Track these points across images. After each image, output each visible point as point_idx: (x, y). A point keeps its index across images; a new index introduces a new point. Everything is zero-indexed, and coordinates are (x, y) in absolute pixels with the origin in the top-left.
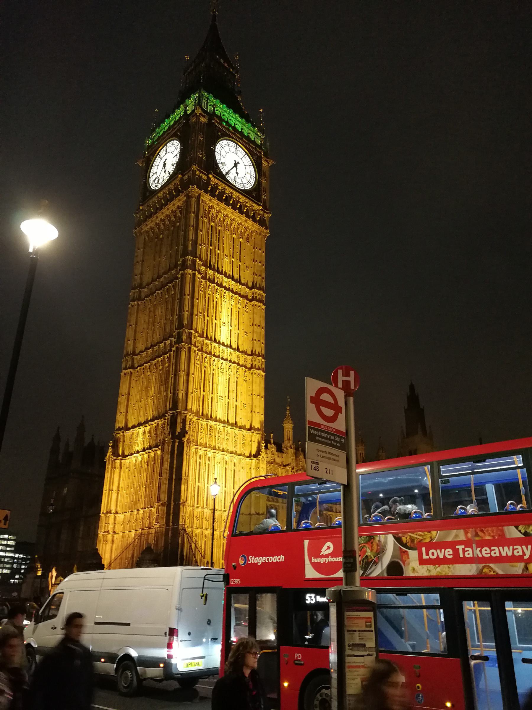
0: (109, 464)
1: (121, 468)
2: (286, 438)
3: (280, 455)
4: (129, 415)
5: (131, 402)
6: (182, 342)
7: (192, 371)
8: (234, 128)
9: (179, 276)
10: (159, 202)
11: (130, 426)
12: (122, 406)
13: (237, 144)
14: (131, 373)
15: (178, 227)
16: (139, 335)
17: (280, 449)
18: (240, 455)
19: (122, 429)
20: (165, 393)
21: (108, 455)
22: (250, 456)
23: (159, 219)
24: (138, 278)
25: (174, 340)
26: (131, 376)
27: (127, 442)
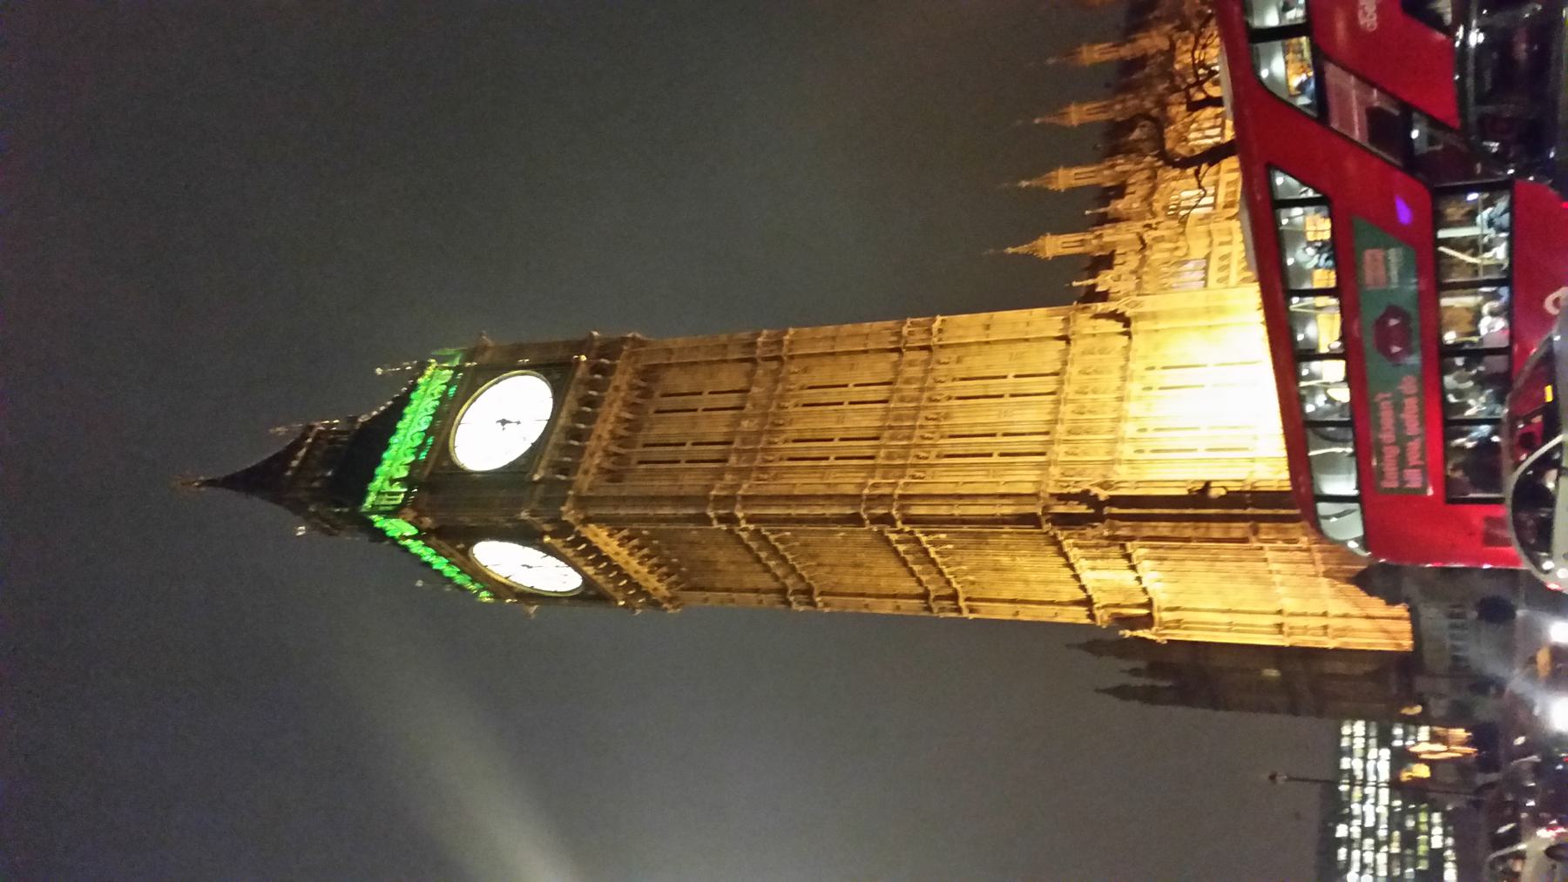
3: (1118, 260)
7: (950, 490)
8: (428, 433)
9: (752, 527)
17: (1105, 261)
18: (1127, 359)
19: (1090, 610)
23: (639, 568)
25: (887, 528)
27: (1119, 599)
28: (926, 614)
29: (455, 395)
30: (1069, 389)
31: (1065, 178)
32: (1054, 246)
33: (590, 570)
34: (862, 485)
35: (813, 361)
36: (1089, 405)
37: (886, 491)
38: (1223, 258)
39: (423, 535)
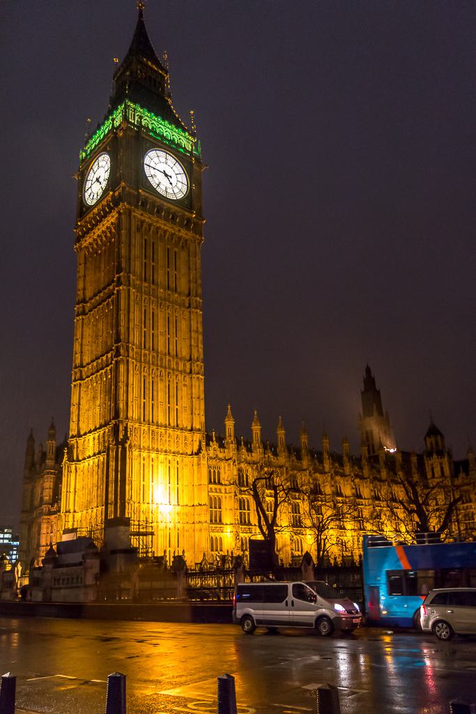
1: (76, 471)
2: (227, 435)
3: (222, 450)
4: (81, 423)
6: (120, 355)
7: (130, 382)
8: (162, 136)
9: (115, 292)
10: (94, 218)
11: (82, 433)
12: (74, 415)
13: (167, 153)
14: (80, 384)
17: (222, 446)
18: (182, 454)
22: (192, 454)
23: (96, 235)
24: (80, 293)
26: (80, 387)
27: (81, 448)
28: (74, 366)
29: (179, 152)
30: (170, 431)
31: (256, 429)
32: (230, 424)
33: (95, 211)
34: (133, 345)
35: (188, 323)
36: (164, 439)
37: (131, 354)
38: (220, 490)
39: (114, 131)
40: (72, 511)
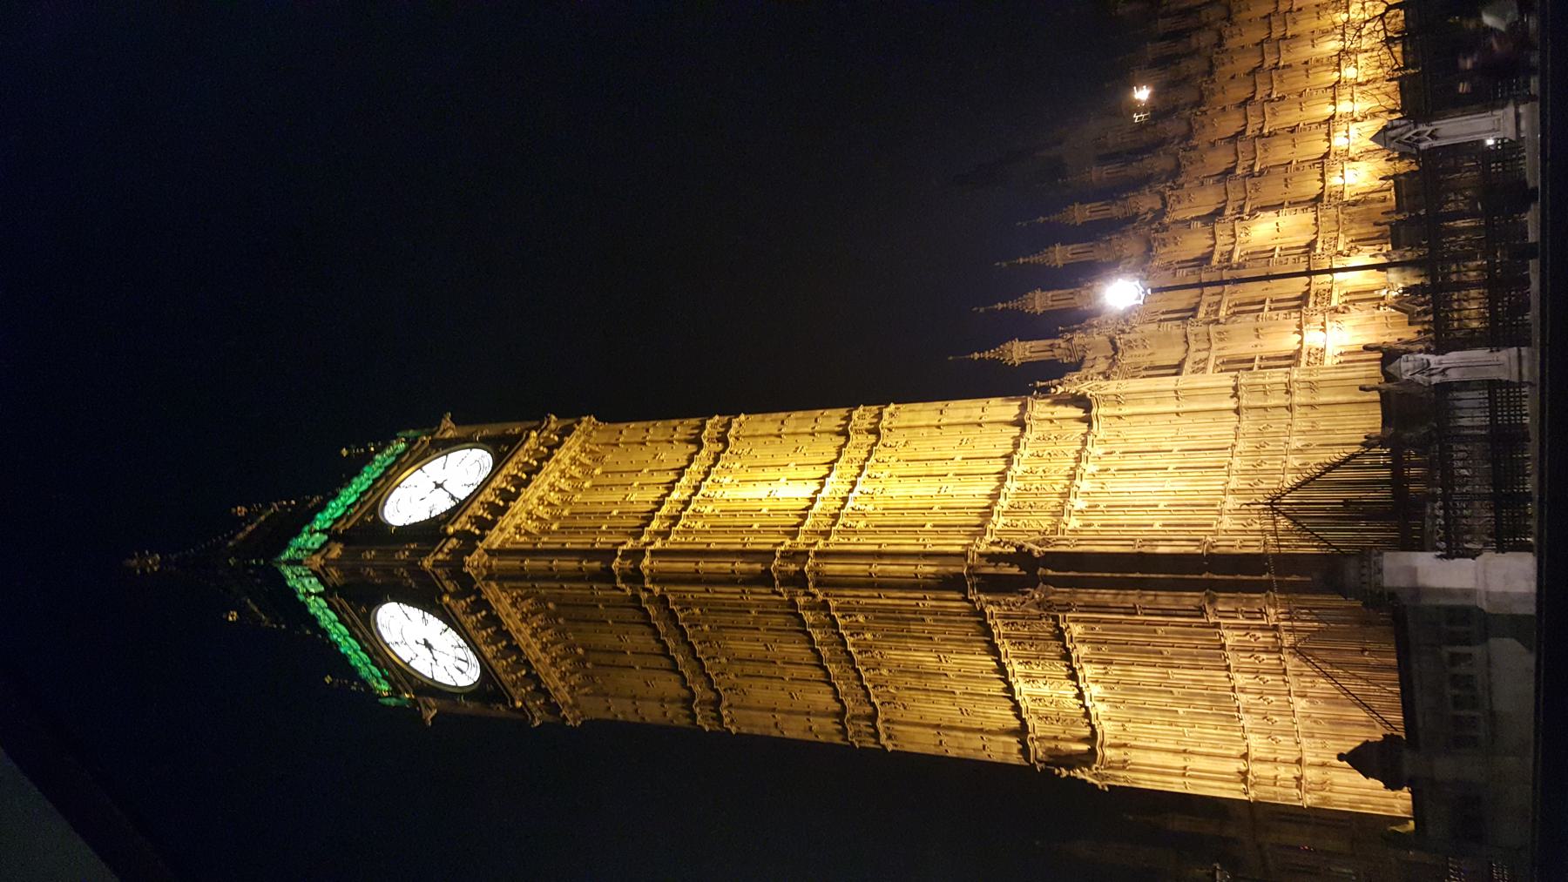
0: (1115, 778)
1: (1125, 745)
3: (1087, 364)
4: (988, 726)
5: (959, 720)
6: (802, 571)
9: (657, 590)
11: (1016, 724)
12: (966, 744)
14: (887, 721)
15: (557, 605)
16: (799, 704)
18: (1084, 443)
19: (1023, 743)
20: (928, 619)
21: (1090, 780)
22: (1088, 420)
23: (541, 656)
27: (1057, 729)
40: (1241, 766)
